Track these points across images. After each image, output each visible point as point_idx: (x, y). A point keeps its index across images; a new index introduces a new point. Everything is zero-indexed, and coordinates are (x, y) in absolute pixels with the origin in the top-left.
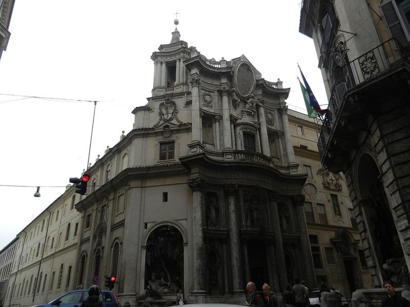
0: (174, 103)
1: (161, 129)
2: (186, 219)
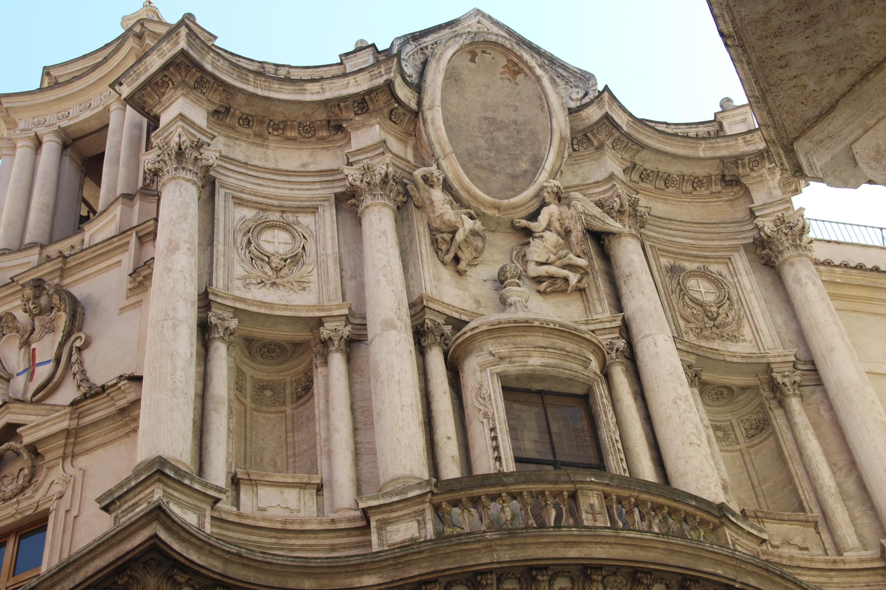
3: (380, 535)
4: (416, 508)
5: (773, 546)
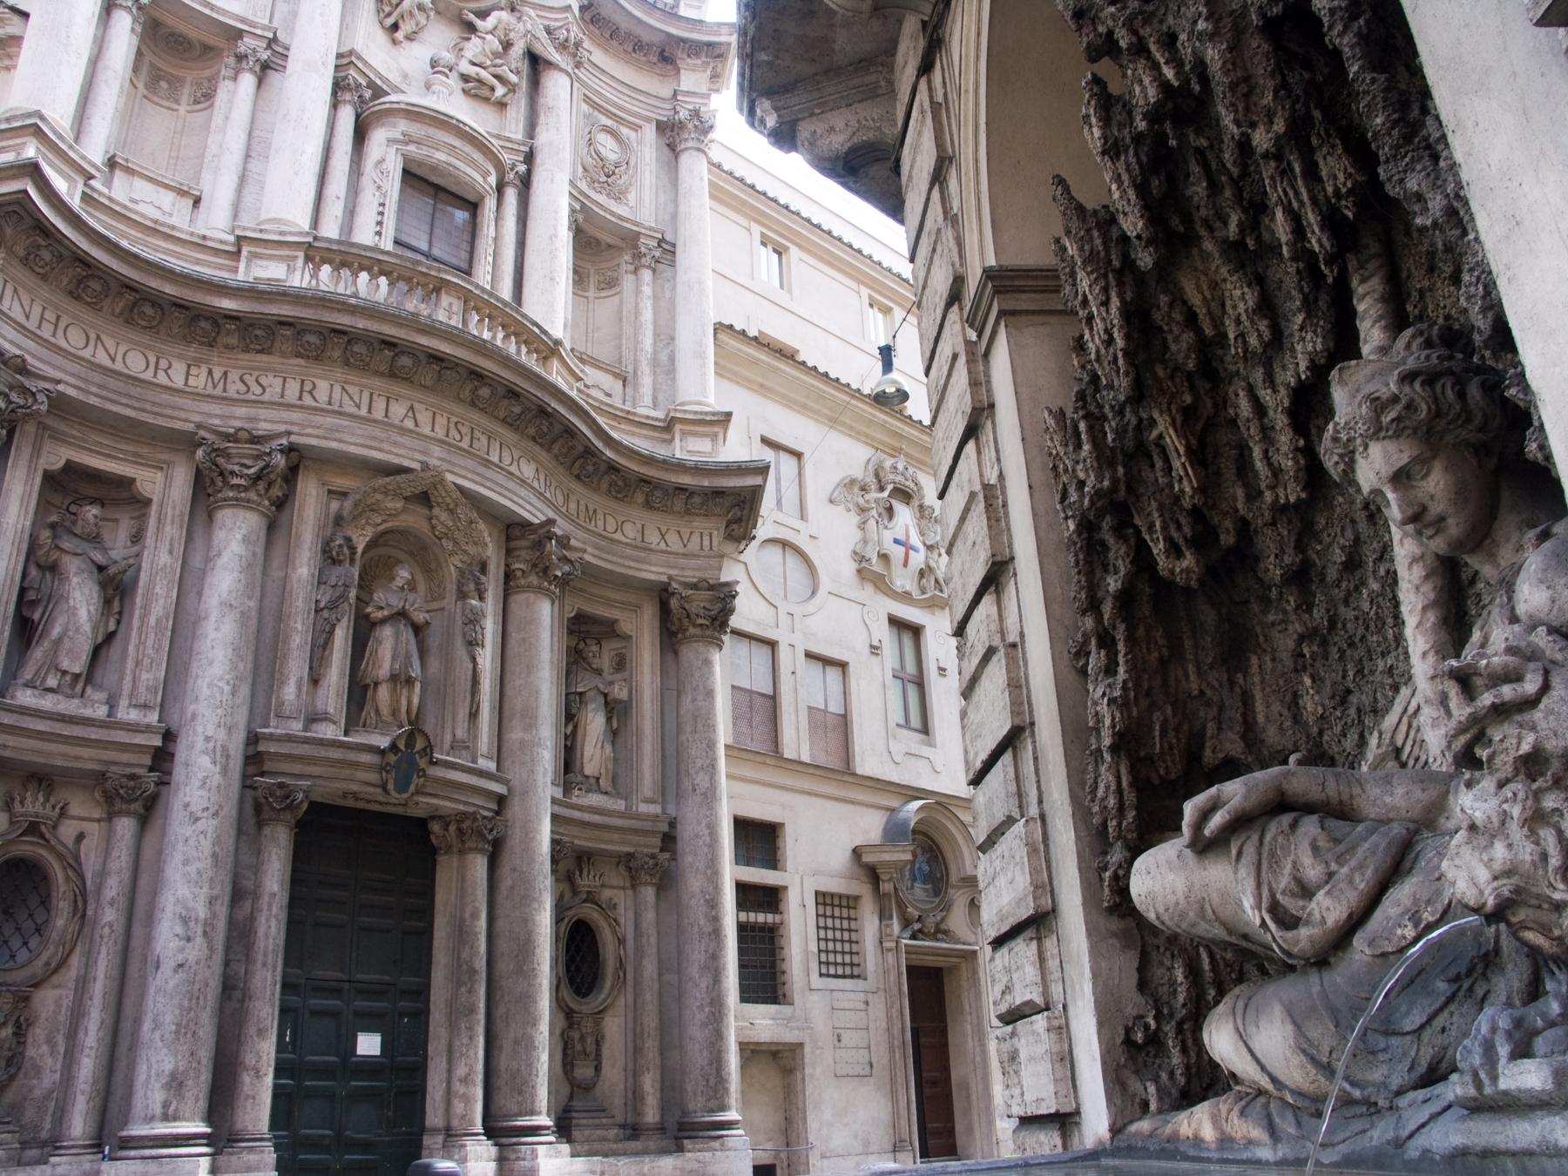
3: (248, 266)
5: (587, 386)
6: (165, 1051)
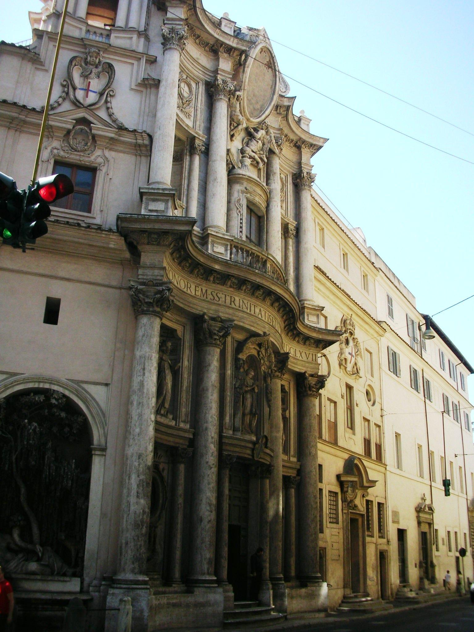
0: (110, 69)
1: (66, 122)
2: (107, 385)
4: (224, 242)
6: (207, 551)
